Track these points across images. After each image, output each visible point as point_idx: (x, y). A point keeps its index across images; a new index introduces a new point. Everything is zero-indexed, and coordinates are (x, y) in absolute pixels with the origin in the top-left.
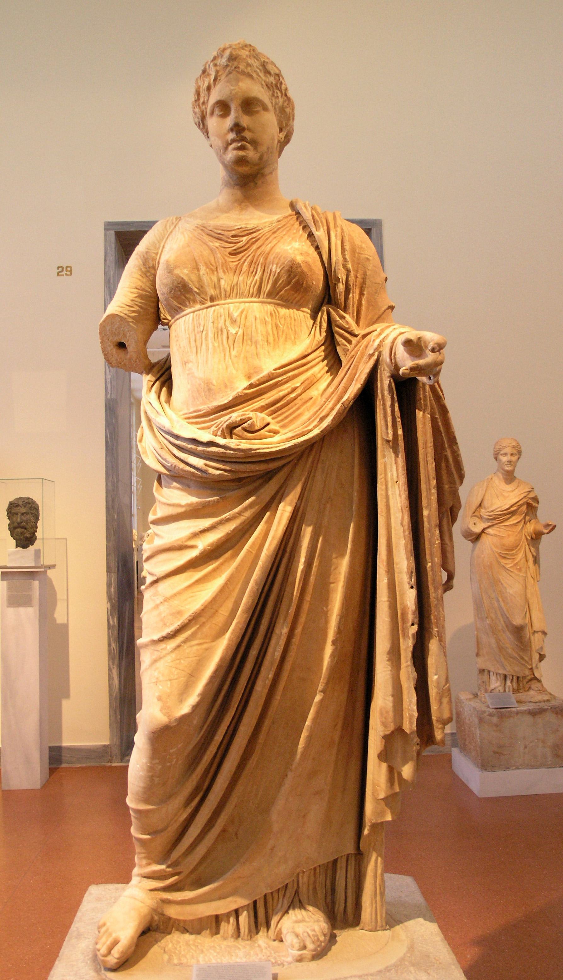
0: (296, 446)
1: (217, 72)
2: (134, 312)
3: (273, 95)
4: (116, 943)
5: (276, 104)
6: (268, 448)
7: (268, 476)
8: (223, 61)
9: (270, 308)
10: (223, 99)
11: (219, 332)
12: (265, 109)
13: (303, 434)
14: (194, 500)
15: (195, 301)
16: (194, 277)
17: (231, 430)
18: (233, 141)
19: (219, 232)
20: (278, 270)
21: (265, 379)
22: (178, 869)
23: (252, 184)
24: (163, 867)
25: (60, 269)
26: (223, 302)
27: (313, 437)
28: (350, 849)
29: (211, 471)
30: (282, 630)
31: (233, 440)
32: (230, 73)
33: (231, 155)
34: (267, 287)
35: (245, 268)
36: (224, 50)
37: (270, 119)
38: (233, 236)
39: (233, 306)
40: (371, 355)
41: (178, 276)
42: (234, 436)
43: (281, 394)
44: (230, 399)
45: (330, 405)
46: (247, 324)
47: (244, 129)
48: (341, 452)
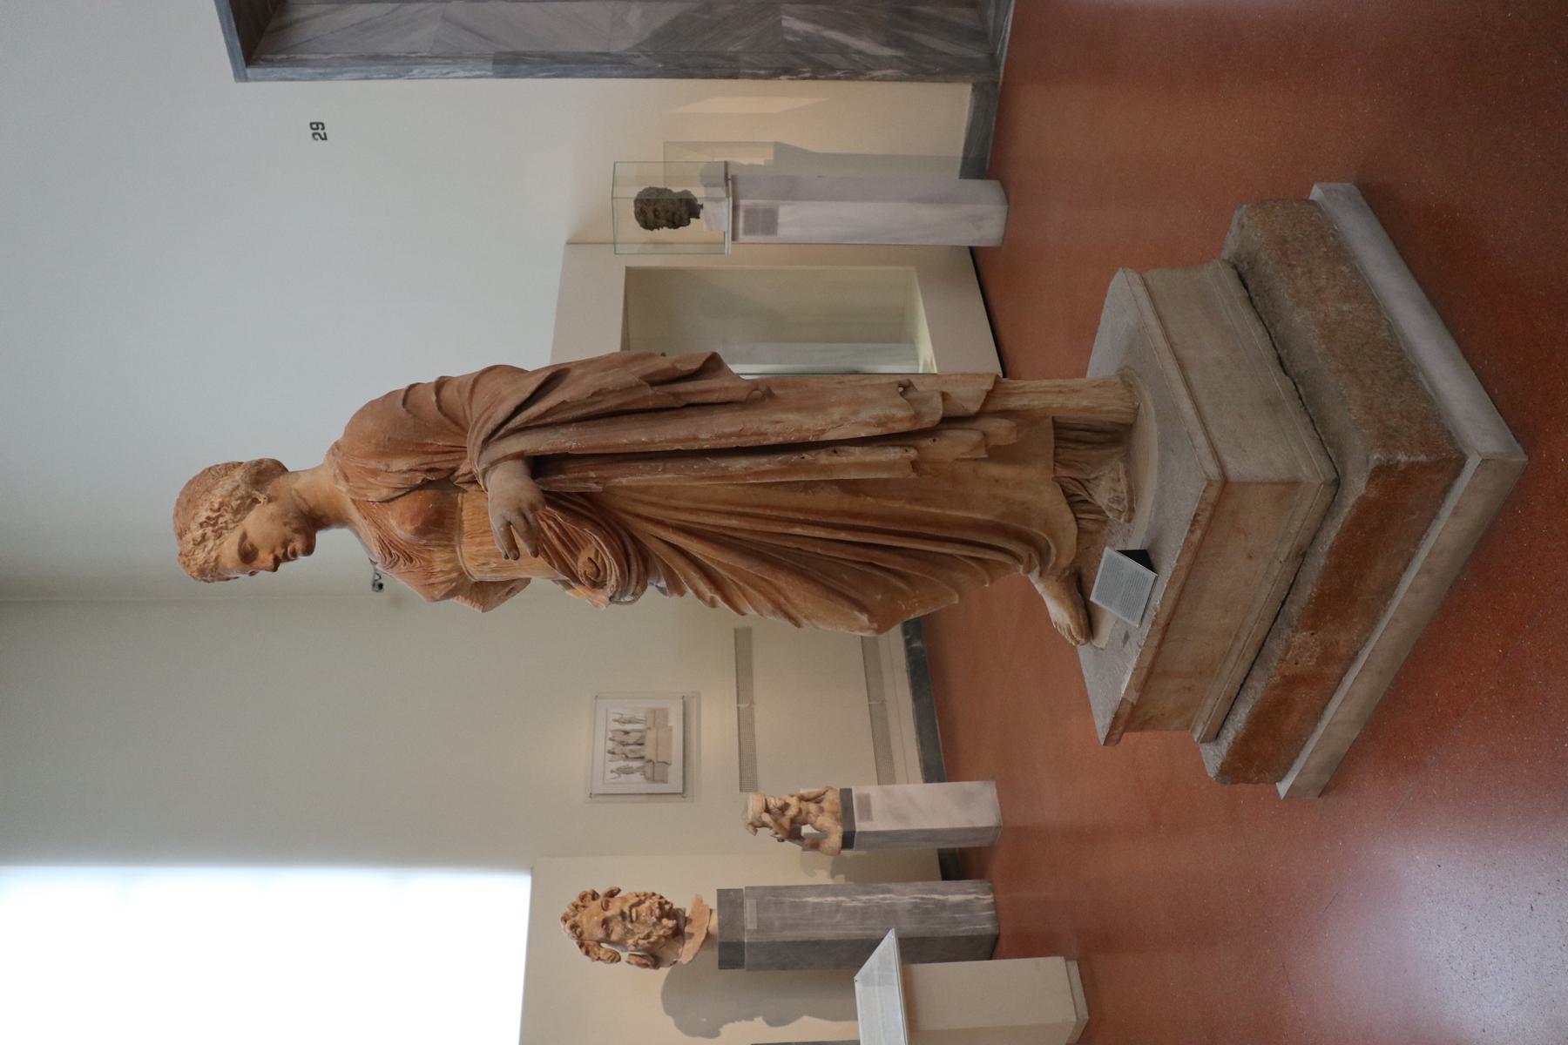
9: (465, 540)
12: (244, 536)
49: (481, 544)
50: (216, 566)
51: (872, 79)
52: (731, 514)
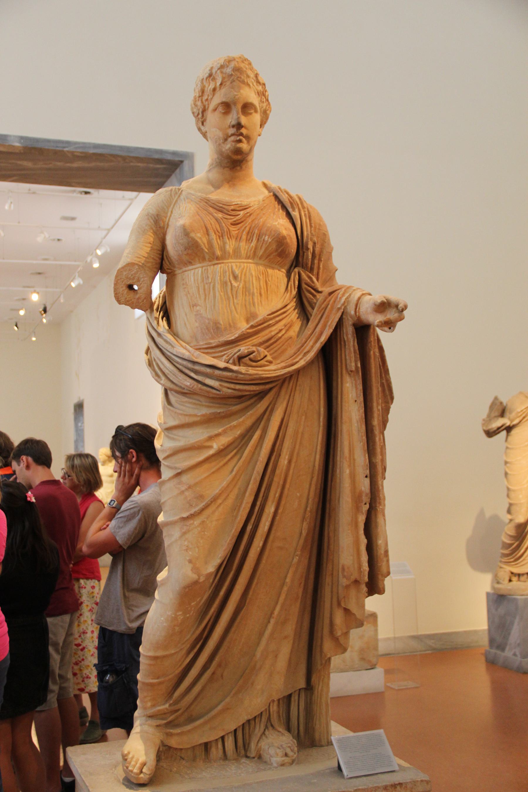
1: (223, 78)
2: (148, 262)
3: (261, 101)
5: (262, 107)
6: (270, 374)
7: (260, 396)
9: (261, 268)
10: (228, 101)
11: (224, 284)
12: (256, 111)
13: (293, 365)
14: (205, 411)
15: (204, 259)
16: (205, 240)
18: (233, 135)
19: (221, 205)
20: (270, 240)
21: (261, 322)
23: (239, 168)
24: (167, 706)
28: (302, 684)
31: (241, 367)
33: (228, 146)
34: (260, 253)
36: (230, 61)
37: (257, 118)
38: (233, 210)
39: (235, 265)
40: (339, 309)
41: (193, 239)
42: (242, 364)
43: (273, 333)
44: (237, 336)
45: (311, 343)
47: (242, 127)
48: (311, 378)
49: (258, 279)
50: (243, 82)
52: (290, 462)
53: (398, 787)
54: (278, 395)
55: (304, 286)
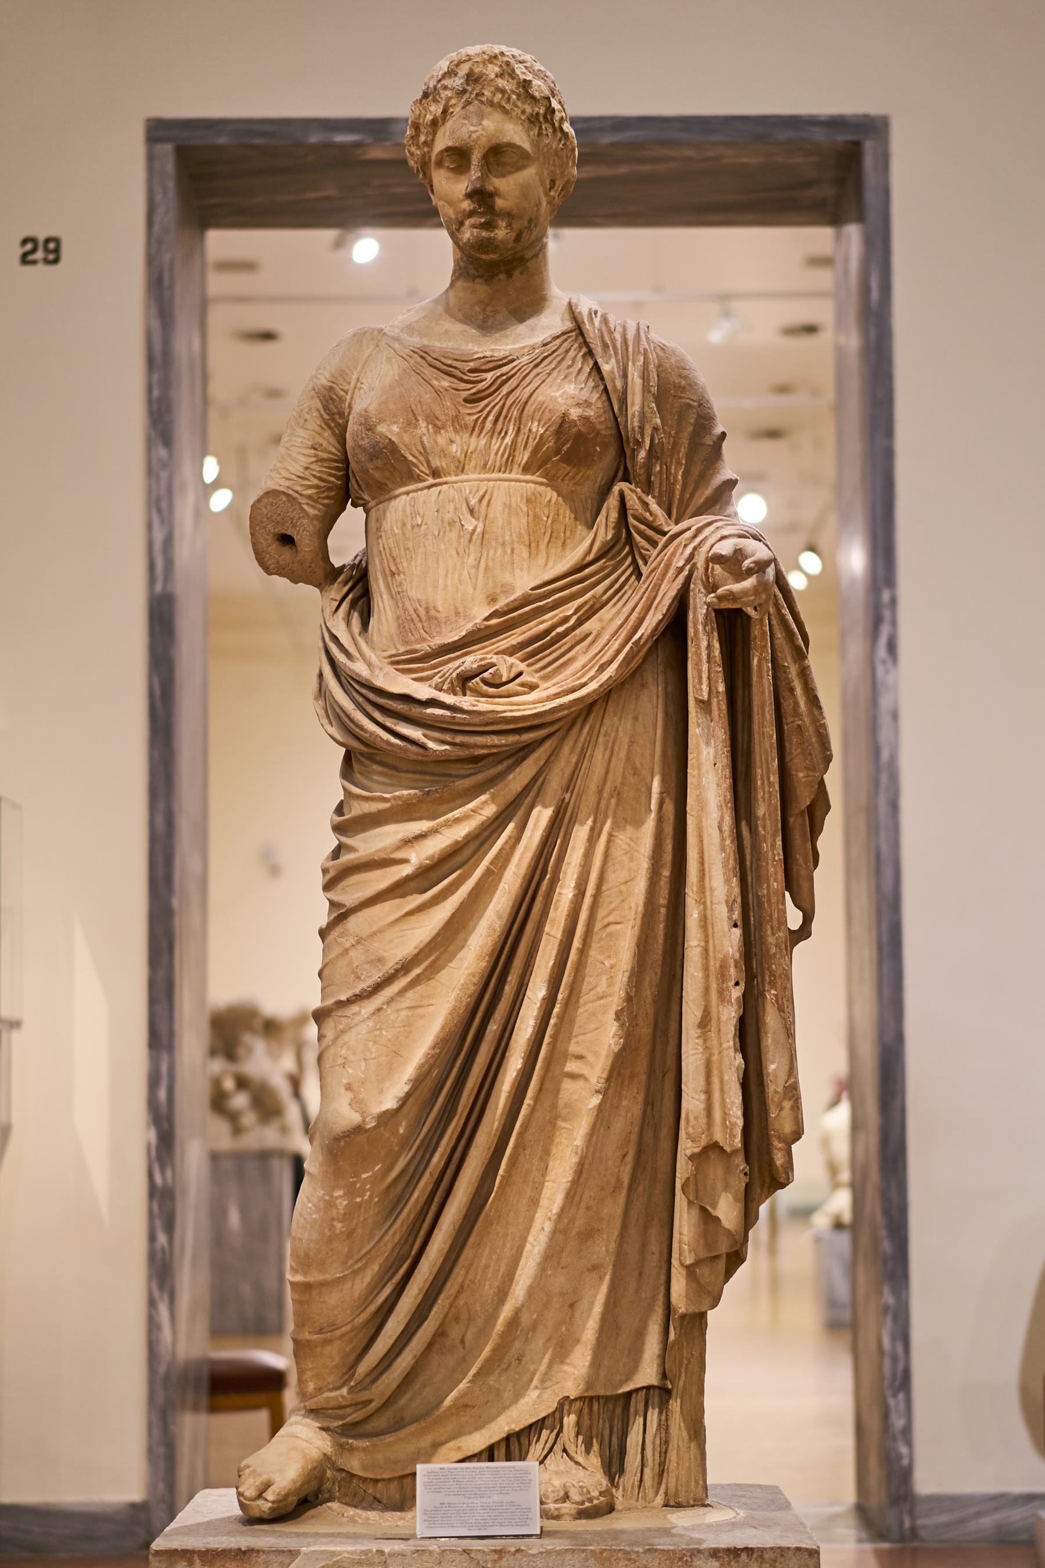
0: (561, 707)
3: (540, 134)
4: (267, 1485)
6: (519, 710)
8: (457, 82)
13: (573, 690)
17: (463, 682)
18: (471, 214)
19: (449, 362)
20: (541, 431)
21: (517, 603)
22: (365, 1396)
25: (29, 246)
26: (453, 478)
27: (588, 695)
29: (431, 745)
30: (537, 991)
31: (466, 698)
32: (468, 103)
35: (489, 425)
38: (471, 371)
40: (681, 570)
42: (468, 693)
44: (463, 634)
45: (616, 646)
46: (491, 515)
48: (636, 719)
51: (152, 1304)
53: (744, 1556)
54: (554, 753)
55: (631, 520)
